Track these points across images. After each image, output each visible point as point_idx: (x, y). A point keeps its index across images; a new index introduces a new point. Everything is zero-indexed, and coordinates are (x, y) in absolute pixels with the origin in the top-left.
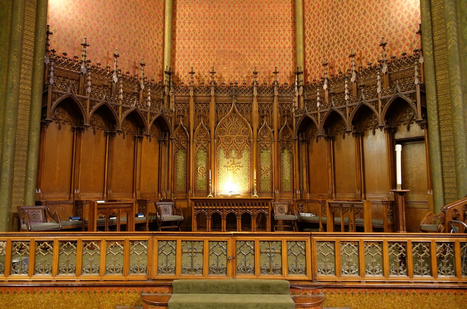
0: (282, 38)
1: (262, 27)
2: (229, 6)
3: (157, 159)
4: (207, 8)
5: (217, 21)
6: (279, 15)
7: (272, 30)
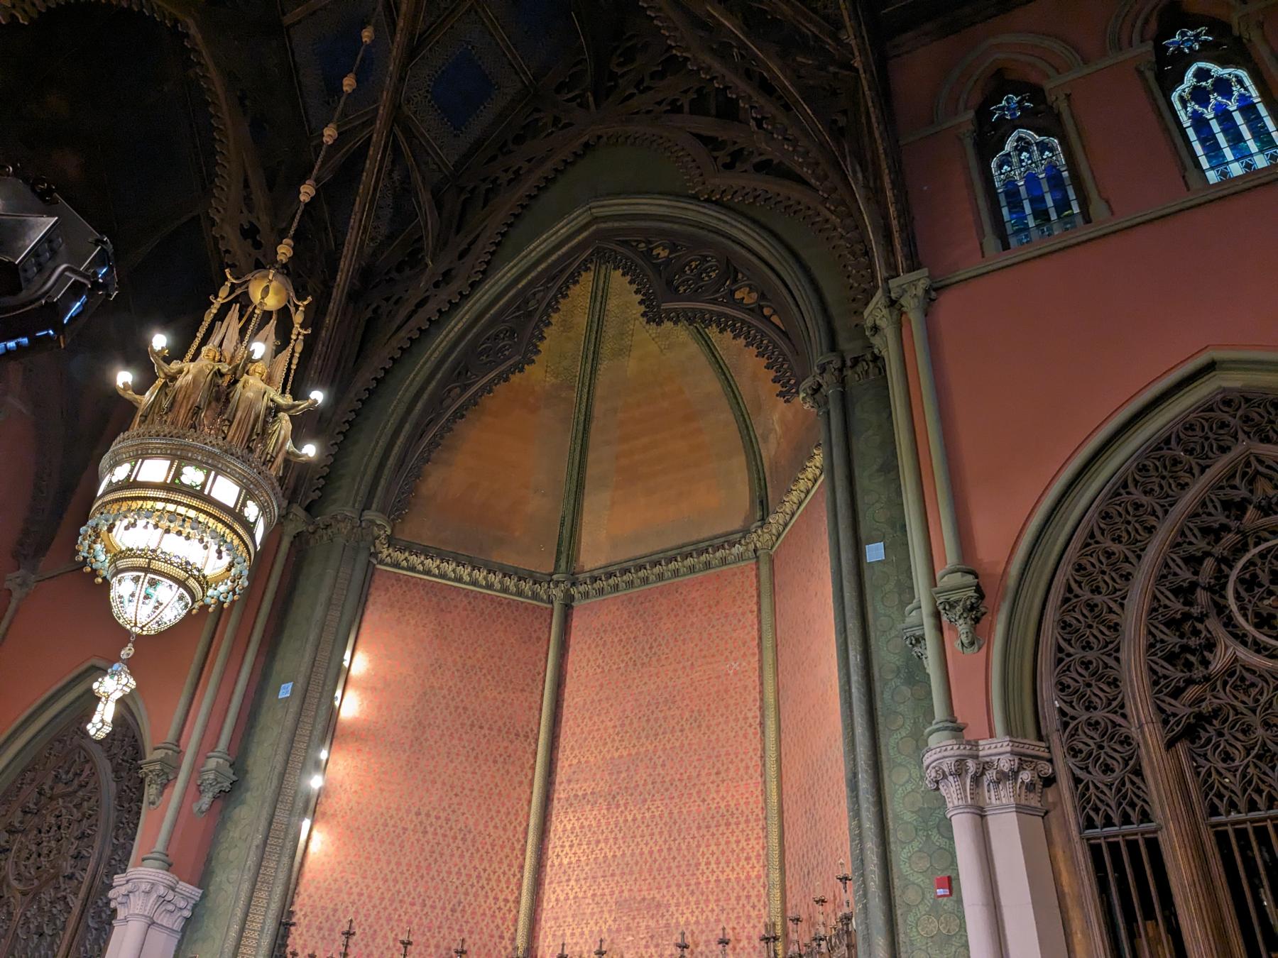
1: (703, 836)
2: (645, 801)
6: (737, 804)
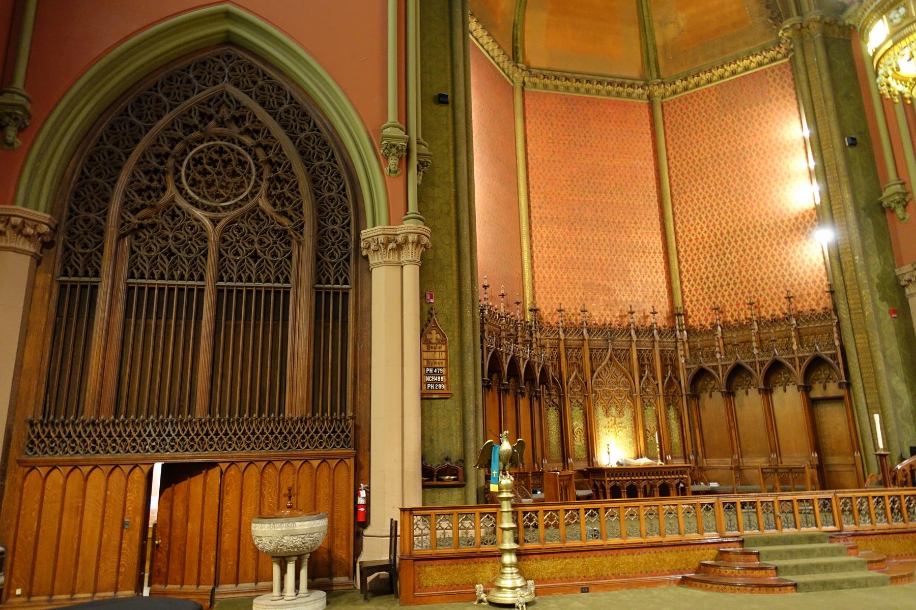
0: (654, 270)
2: (593, 230)
3: (529, 418)
4: (567, 230)
5: (580, 247)
6: (648, 243)
7: (642, 261)
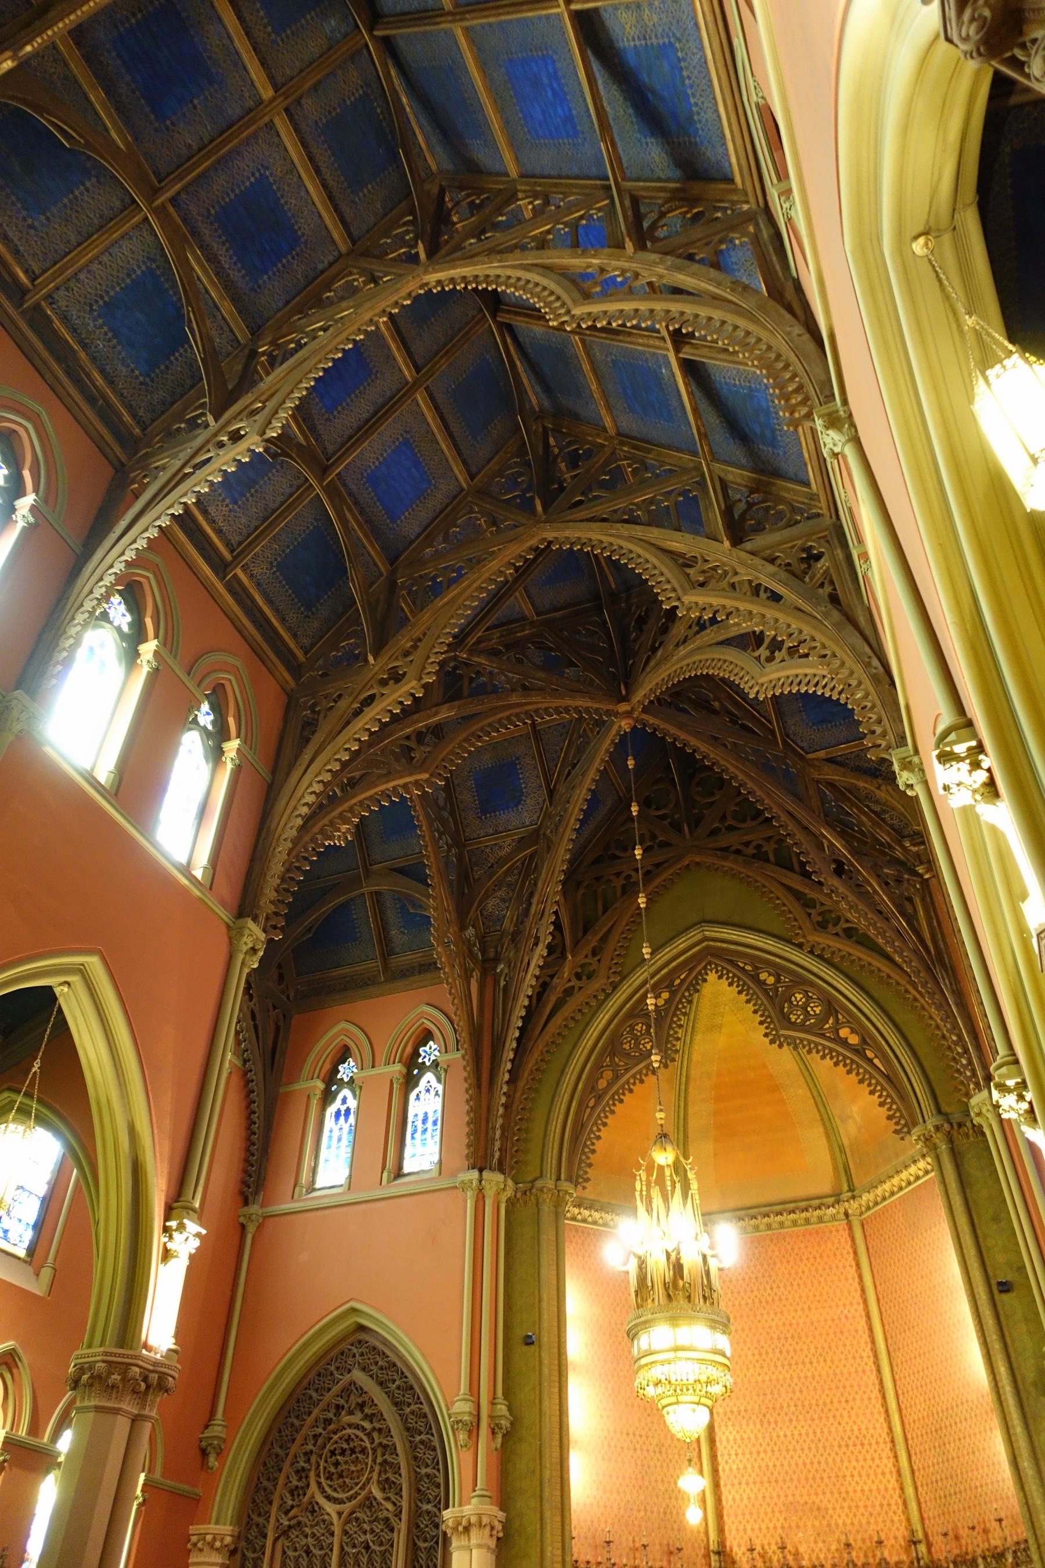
0: (879, 1471)
4: (758, 1426)
6: (867, 1429)
7: (861, 1458)
